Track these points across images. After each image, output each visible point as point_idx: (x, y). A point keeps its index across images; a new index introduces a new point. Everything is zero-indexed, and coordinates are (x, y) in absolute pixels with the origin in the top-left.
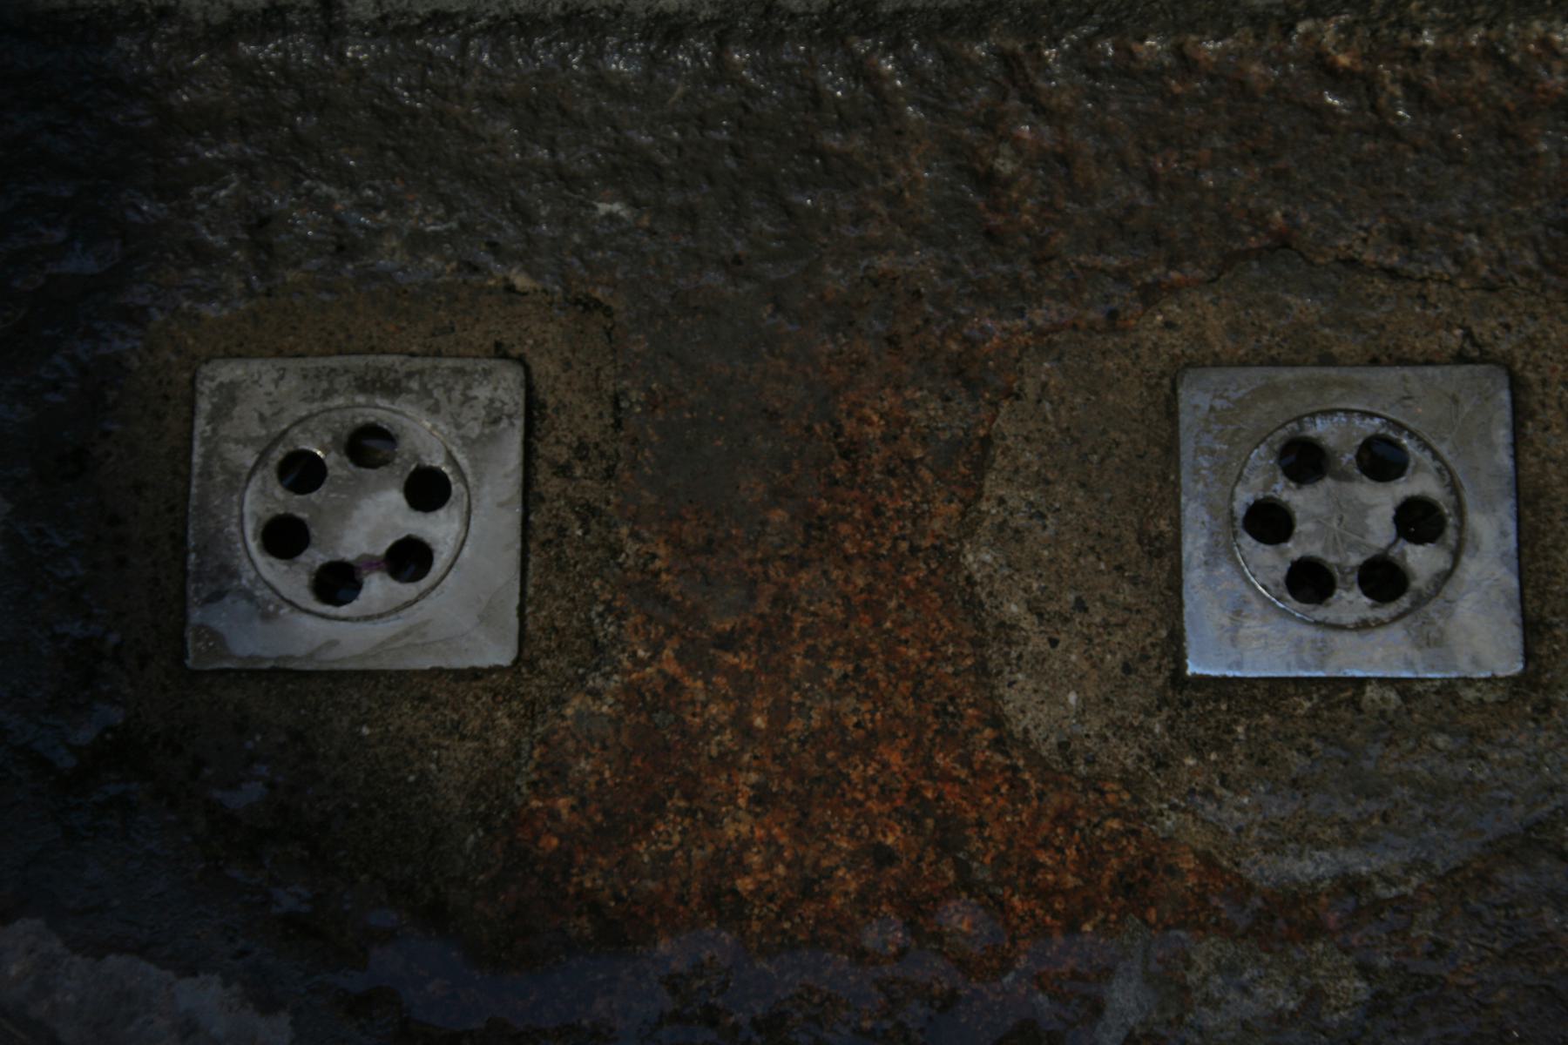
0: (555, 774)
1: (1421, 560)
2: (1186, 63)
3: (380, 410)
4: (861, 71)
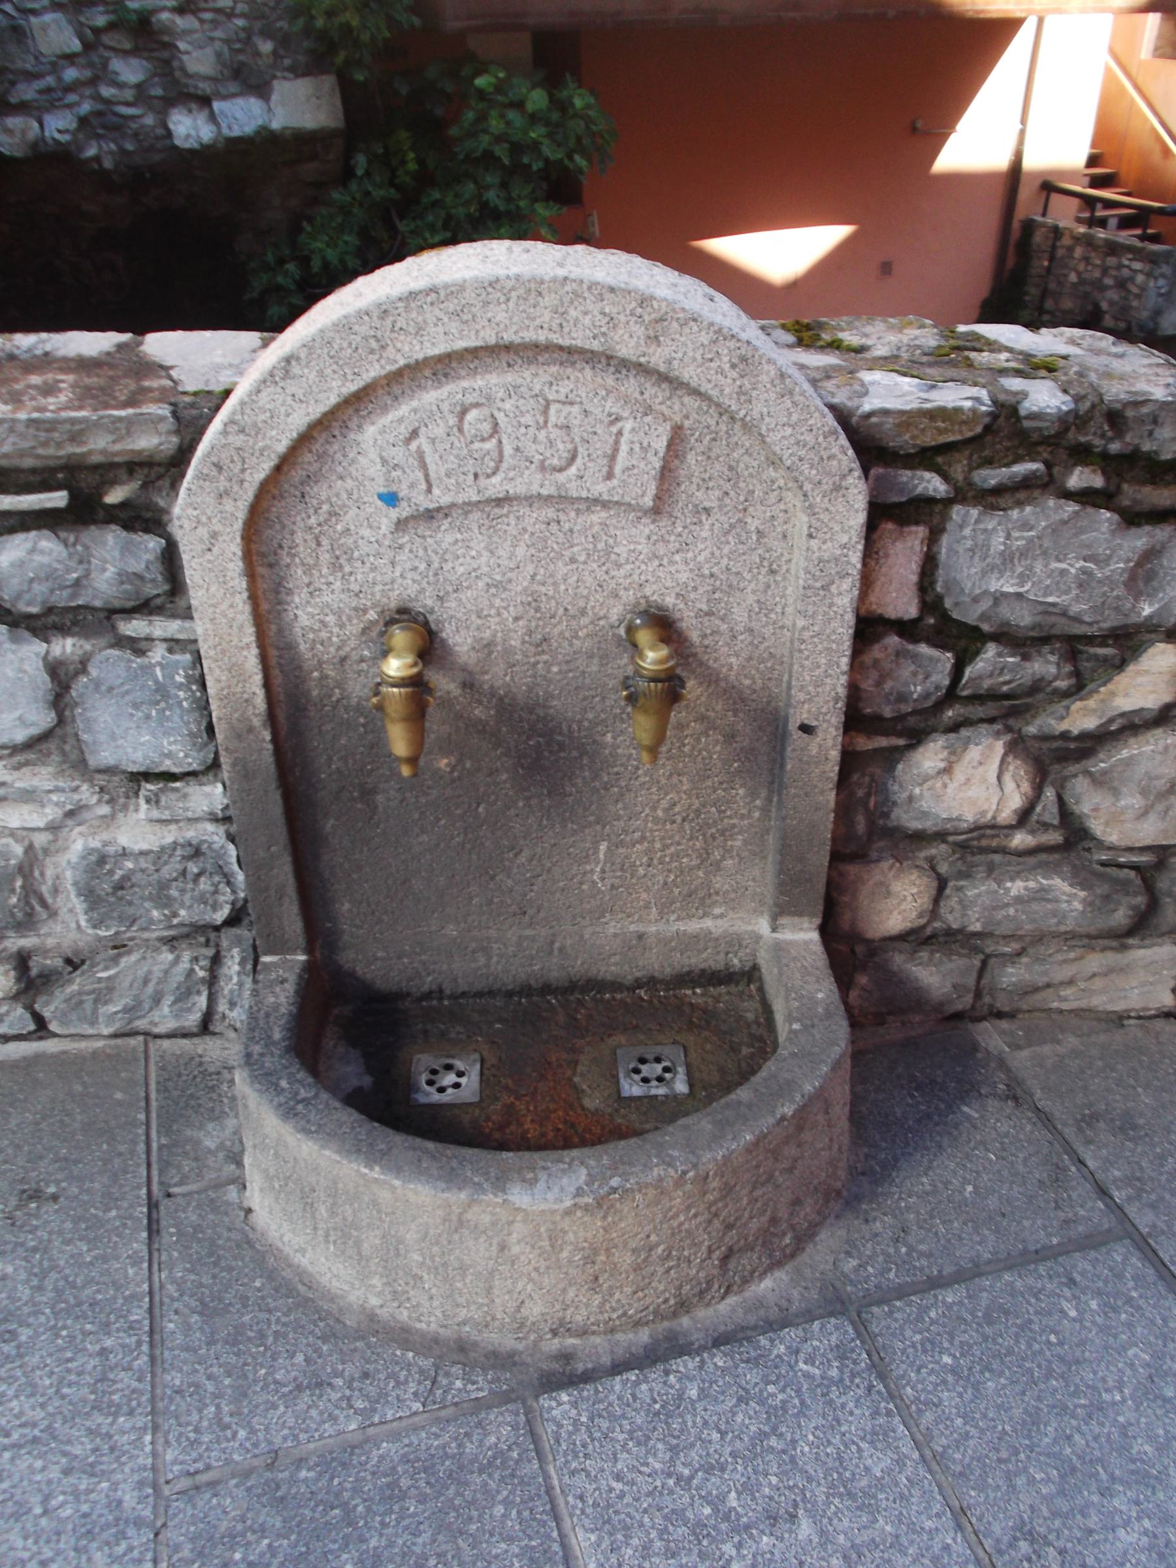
0: (488, 1119)
1: (668, 1076)
2: (614, 999)
3: (450, 1061)
4: (549, 1002)
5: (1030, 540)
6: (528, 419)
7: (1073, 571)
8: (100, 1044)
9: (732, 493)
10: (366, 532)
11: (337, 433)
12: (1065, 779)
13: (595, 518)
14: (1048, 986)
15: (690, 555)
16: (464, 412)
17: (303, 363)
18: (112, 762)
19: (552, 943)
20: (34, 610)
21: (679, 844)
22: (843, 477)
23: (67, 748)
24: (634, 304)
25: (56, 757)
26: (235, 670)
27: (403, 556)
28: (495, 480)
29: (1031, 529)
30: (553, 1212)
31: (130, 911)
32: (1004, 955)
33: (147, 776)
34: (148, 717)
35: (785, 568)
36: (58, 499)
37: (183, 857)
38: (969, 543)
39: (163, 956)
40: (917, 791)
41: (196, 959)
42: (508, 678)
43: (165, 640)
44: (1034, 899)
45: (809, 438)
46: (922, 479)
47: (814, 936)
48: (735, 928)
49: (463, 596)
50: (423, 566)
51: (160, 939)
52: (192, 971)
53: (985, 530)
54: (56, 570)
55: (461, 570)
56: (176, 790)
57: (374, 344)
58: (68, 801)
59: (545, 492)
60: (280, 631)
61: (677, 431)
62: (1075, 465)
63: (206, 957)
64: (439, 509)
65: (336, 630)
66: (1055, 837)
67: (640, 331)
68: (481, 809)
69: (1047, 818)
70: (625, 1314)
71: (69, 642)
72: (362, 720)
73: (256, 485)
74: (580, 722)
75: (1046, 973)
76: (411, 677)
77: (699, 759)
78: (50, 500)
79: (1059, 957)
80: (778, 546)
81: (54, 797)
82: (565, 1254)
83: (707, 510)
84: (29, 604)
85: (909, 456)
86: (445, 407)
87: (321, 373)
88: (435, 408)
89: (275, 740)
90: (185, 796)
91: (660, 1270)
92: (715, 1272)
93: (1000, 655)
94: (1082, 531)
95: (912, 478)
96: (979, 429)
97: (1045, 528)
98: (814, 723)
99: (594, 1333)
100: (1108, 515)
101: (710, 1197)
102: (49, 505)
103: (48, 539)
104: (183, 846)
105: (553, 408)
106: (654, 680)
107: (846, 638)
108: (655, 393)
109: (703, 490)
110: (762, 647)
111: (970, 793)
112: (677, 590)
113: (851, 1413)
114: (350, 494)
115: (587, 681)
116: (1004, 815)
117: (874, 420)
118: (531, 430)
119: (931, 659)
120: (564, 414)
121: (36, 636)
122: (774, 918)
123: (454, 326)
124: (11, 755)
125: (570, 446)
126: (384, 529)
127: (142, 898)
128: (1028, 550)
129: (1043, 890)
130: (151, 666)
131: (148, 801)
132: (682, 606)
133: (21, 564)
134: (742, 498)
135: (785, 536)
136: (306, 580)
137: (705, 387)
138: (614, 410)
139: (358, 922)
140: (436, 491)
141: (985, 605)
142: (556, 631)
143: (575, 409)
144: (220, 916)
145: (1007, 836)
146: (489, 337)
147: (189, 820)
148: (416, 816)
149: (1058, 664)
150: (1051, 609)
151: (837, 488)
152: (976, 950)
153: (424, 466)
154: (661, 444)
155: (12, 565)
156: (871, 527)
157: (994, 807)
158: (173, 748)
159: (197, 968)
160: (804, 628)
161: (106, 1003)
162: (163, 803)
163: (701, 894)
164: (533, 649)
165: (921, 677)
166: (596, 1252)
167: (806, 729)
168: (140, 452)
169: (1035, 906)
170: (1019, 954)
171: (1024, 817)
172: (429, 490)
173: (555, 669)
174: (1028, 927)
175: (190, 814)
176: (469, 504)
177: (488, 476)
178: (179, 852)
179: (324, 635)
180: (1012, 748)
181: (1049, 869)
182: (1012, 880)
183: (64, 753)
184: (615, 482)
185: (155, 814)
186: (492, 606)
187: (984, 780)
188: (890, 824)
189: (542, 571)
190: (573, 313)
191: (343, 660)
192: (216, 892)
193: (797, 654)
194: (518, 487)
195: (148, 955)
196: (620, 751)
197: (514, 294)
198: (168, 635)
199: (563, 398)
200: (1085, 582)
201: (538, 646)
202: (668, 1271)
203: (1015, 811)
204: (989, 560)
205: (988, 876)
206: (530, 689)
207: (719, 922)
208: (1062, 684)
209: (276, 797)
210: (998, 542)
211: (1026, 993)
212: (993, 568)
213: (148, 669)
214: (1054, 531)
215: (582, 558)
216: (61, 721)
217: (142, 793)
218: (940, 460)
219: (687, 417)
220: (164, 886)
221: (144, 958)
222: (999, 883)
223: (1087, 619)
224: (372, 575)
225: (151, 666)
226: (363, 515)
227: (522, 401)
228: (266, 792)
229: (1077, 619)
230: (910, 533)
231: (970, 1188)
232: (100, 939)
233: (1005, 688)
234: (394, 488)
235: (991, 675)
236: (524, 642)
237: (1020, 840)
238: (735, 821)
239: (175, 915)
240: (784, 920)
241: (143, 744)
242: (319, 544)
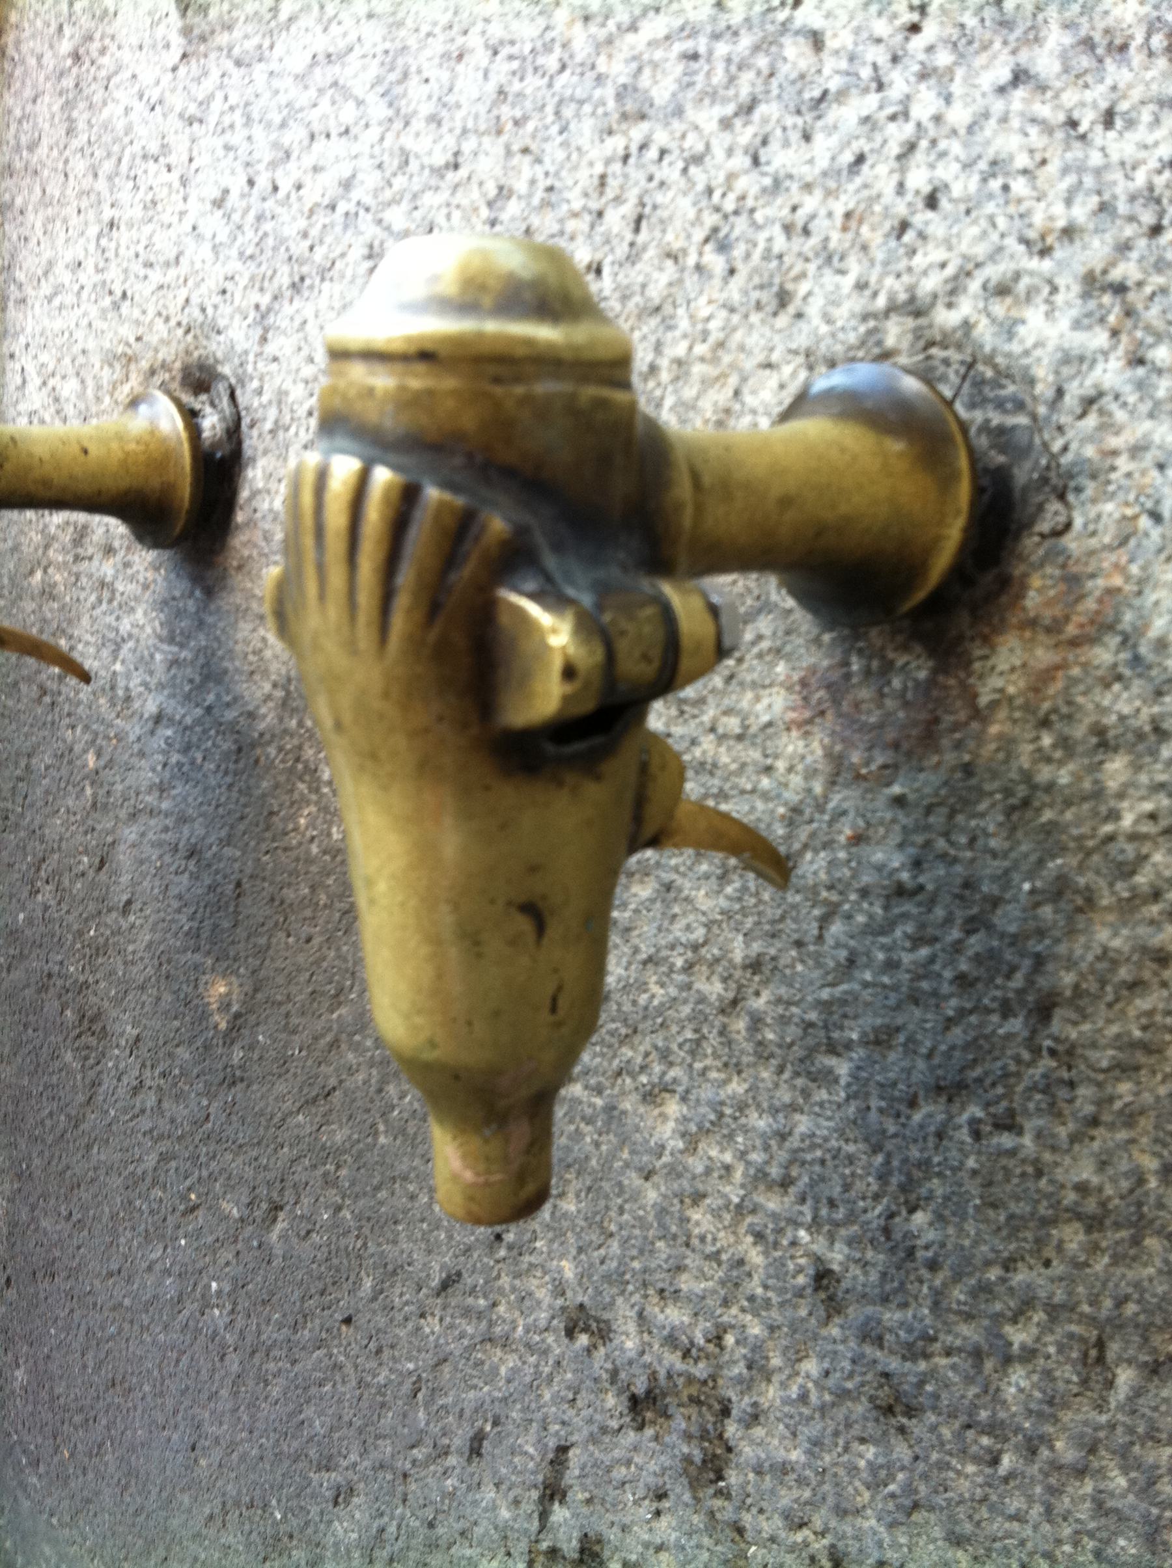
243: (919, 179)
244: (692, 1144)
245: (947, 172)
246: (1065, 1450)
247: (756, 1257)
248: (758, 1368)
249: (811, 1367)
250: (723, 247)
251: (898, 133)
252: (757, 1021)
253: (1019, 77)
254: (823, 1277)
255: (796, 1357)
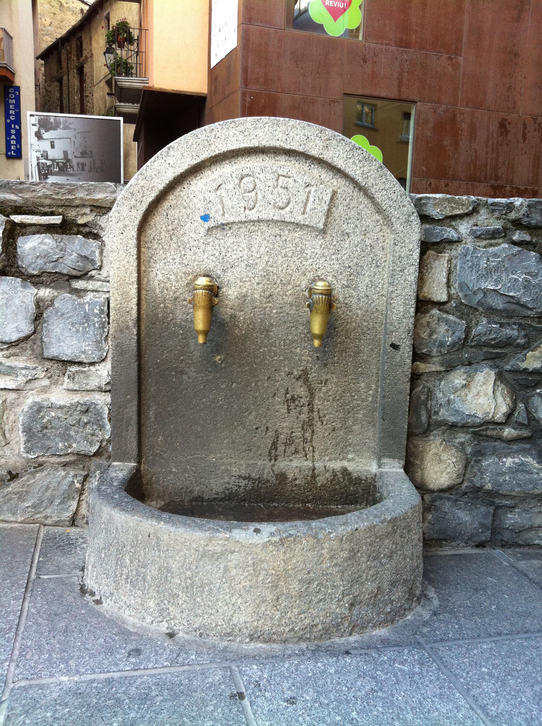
4: (260, 506)
5: (499, 262)
6: (270, 183)
7: (521, 280)
8: (17, 525)
9: (359, 226)
10: (193, 235)
11: (185, 187)
12: (529, 398)
13: (297, 235)
14: (531, 528)
15: (339, 256)
16: (242, 178)
17: (175, 150)
18: (56, 354)
19: (264, 469)
20: (35, 272)
21: (331, 414)
22: (410, 216)
23: (35, 347)
24: (318, 132)
25: (29, 352)
26: (125, 295)
27: (209, 248)
28: (254, 211)
29: (498, 257)
30: (256, 545)
31: (48, 443)
32: (506, 506)
33: (72, 363)
34: (78, 331)
35: (383, 264)
36: (57, 220)
37: (81, 412)
38: (470, 264)
39: (59, 473)
40: (452, 397)
41: (75, 476)
42: (252, 315)
43: (93, 291)
44: (517, 471)
45: (394, 196)
46: (446, 231)
47: (402, 471)
48: (359, 468)
49: (234, 270)
50: (217, 254)
51: (58, 463)
52: (73, 482)
53: (477, 257)
54: (50, 253)
55: (234, 257)
56: (84, 372)
57: (206, 144)
58: (30, 374)
59: (275, 218)
60: (149, 281)
61: (334, 193)
62: (516, 230)
63: (81, 475)
64: (227, 224)
65: (174, 283)
66: (526, 433)
67: (320, 144)
68: (233, 386)
69: (521, 420)
70: (292, 630)
71: (48, 290)
72: (181, 332)
73: (147, 204)
74: (285, 340)
75: (530, 519)
76: (208, 286)
77: (342, 364)
78: (54, 219)
79: (536, 510)
80: (380, 254)
81: (24, 372)
82: (261, 578)
83: (348, 235)
84: (34, 269)
85: (439, 220)
86: (234, 175)
87: (182, 155)
88: (229, 175)
89: (139, 334)
90: (88, 376)
91: (315, 600)
92: (347, 612)
93: (489, 323)
94: (522, 261)
95: (442, 230)
96: (471, 208)
97: (505, 257)
98: (398, 344)
99: (274, 641)
100: (534, 254)
101: (345, 554)
102: (53, 222)
103: (49, 238)
104: (82, 405)
105: (281, 178)
106: (322, 294)
107: (413, 298)
108: (326, 175)
109: (346, 224)
110: (373, 305)
111: (480, 401)
112: (333, 273)
113: (427, 686)
114: (188, 216)
115: (289, 318)
116: (498, 416)
117: (423, 201)
118: (271, 188)
119: (455, 323)
120: (285, 182)
121: (34, 286)
122: (379, 459)
123: (241, 138)
124: (8, 349)
125: (287, 197)
126: (202, 234)
127: (55, 435)
128: (498, 267)
129: (523, 464)
130: (84, 304)
131: (69, 378)
132: (335, 282)
133: (34, 249)
134: (363, 229)
135: (383, 249)
136: (164, 256)
137: (348, 171)
138: (307, 181)
139: (164, 449)
140: (226, 215)
141: (480, 296)
142: (276, 291)
143: (291, 180)
144: (94, 449)
145: (501, 429)
146: (254, 143)
147: (88, 391)
148: (202, 387)
149: (518, 330)
150: (512, 300)
151: (408, 221)
152: (492, 504)
153: (222, 202)
154: (327, 198)
155: (30, 249)
156: (423, 253)
157: (493, 411)
158: (87, 348)
159: (76, 481)
160: (392, 292)
161: (24, 501)
162: (76, 380)
163: (342, 445)
164: (265, 300)
165: (450, 333)
166: (279, 580)
167: (395, 346)
168: (98, 200)
169: (520, 476)
170: (514, 507)
171: (509, 415)
172: (223, 215)
173: (275, 311)
174: (518, 489)
175: (88, 387)
176: (240, 222)
177: (250, 210)
178: (79, 409)
179: (168, 285)
180: (500, 377)
181: (524, 452)
182: (506, 457)
183: (33, 350)
184: (307, 216)
185: (71, 386)
186: (247, 276)
187: (486, 394)
188: (439, 419)
189: (271, 260)
190: (291, 134)
191: (176, 299)
192: (93, 435)
193: (389, 306)
194: (263, 216)
195: (51, 472)
196: (303, 358)
197: (267, 125)
198: (95, 288)
199: (285, 174)
200: (527, 285)
201: (267, 298)
202: (318, 602)
203: (504, 414)
204: (480, 272)
205: (493, 454)
206: (262, 321)
207: (351, 463)
208: (521, 341)
209: (135, 365)
210: (483, 263)
211: (520, 532)
212: (482, 276)
213: (82, 305)
214: (510, 259)
215: (290, 255)
216: (34, 333)
217: (68, 373)
218: (454, 223)
219: (339, 188)
220: (67, 429)
221: (49, 474)
222: (500, 458)
223: (530, 306)
224: (194, 257)
225: (84, 304)
226: (193, 226)
227: (267, 174)
228: (130, 363)
229: (524, 306)
230: (442, 256)
231: (494, 607)
232: (28, 460)
233: (493, 343)
234: (207, 212)
235: (485, 334)
236: (261, 296)
237: (508, 432)
238: (360, 402)
239: (70, 446)
240: (385, 460)
241: (72, 346)
242: (171, 239)
243: (317, 266)
244: (301, 351)
245: (320, 266)
246: (340, 362)
247: (310, 359)
248: (311, 369)
249: (317, 366)
250: (298, 270)
251: (315, 263)
252: (308, 337)
253: (326, 260)
254: (317, 357)
255: (315, 366)
